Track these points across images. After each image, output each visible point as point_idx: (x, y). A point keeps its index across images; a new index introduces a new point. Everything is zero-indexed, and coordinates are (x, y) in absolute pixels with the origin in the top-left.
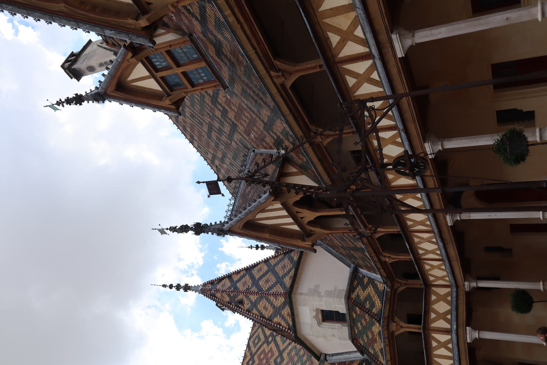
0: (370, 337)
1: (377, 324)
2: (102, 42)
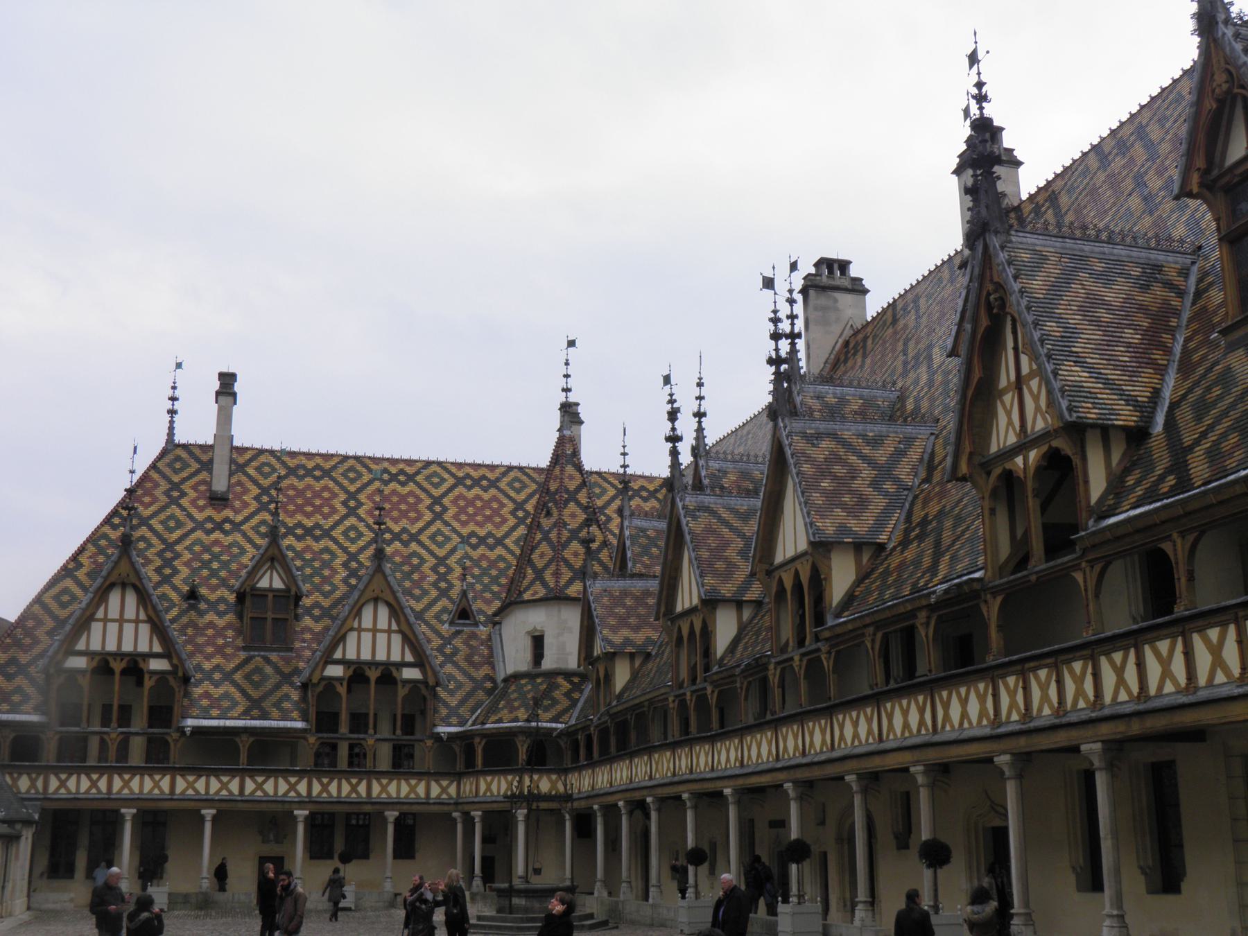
0: (516, 704)
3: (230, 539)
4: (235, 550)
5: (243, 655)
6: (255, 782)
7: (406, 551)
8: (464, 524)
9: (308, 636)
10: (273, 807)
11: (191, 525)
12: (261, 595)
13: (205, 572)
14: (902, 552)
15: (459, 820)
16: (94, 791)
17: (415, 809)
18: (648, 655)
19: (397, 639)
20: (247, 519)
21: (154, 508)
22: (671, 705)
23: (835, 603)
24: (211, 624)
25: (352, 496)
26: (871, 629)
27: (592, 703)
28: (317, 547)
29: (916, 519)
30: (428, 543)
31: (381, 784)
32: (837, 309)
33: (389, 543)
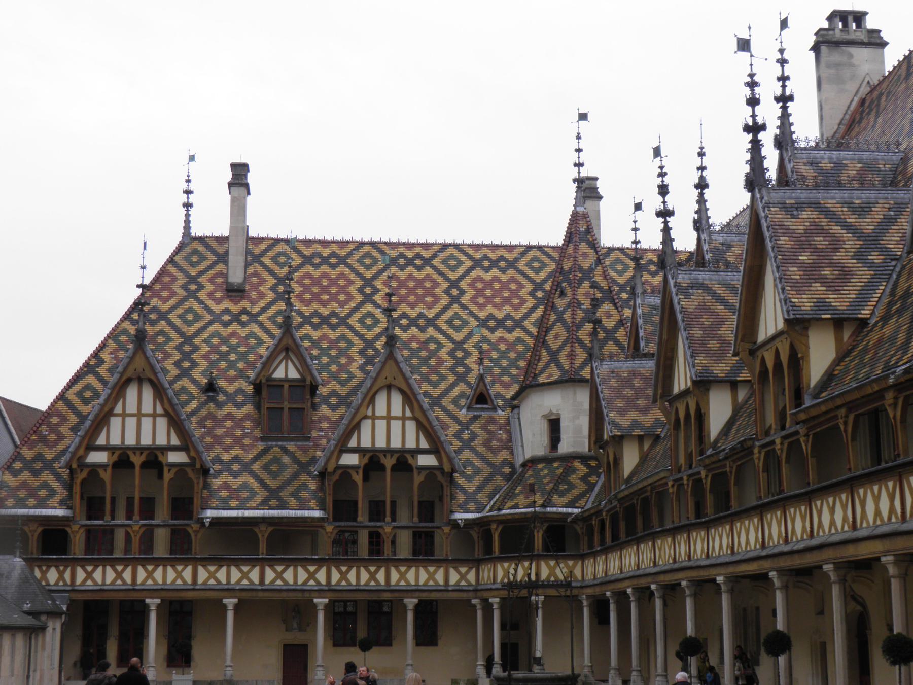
1: (541, 502)
2: (872, 83)
3: (247, 330)
4: (253, 341)
5: (261, 445)
6: (275, 571)
7: (422, 337)
8: (482, 307)
9: (325, 425)
10: (292, 595)
11: (208, 317)
12: (277, 386)
13: (223, 364)
14: (882, 328)
15: (478, 607)
16: (119, 582)
17: (434, 596)
18: (657, 438)
19: (411, 426)
20: (263, 310)
21: (172, 302)
22: (671, 490)
23: (813, 384)
24: (229, 416)
25: (368, 282)
26: (843, 411)
27: (606, 487)
28: (333, 335)
29: (900, 292)
30: (445, 327)
31: (399, 571)
32: (852, 65)
33: (405, 329)
